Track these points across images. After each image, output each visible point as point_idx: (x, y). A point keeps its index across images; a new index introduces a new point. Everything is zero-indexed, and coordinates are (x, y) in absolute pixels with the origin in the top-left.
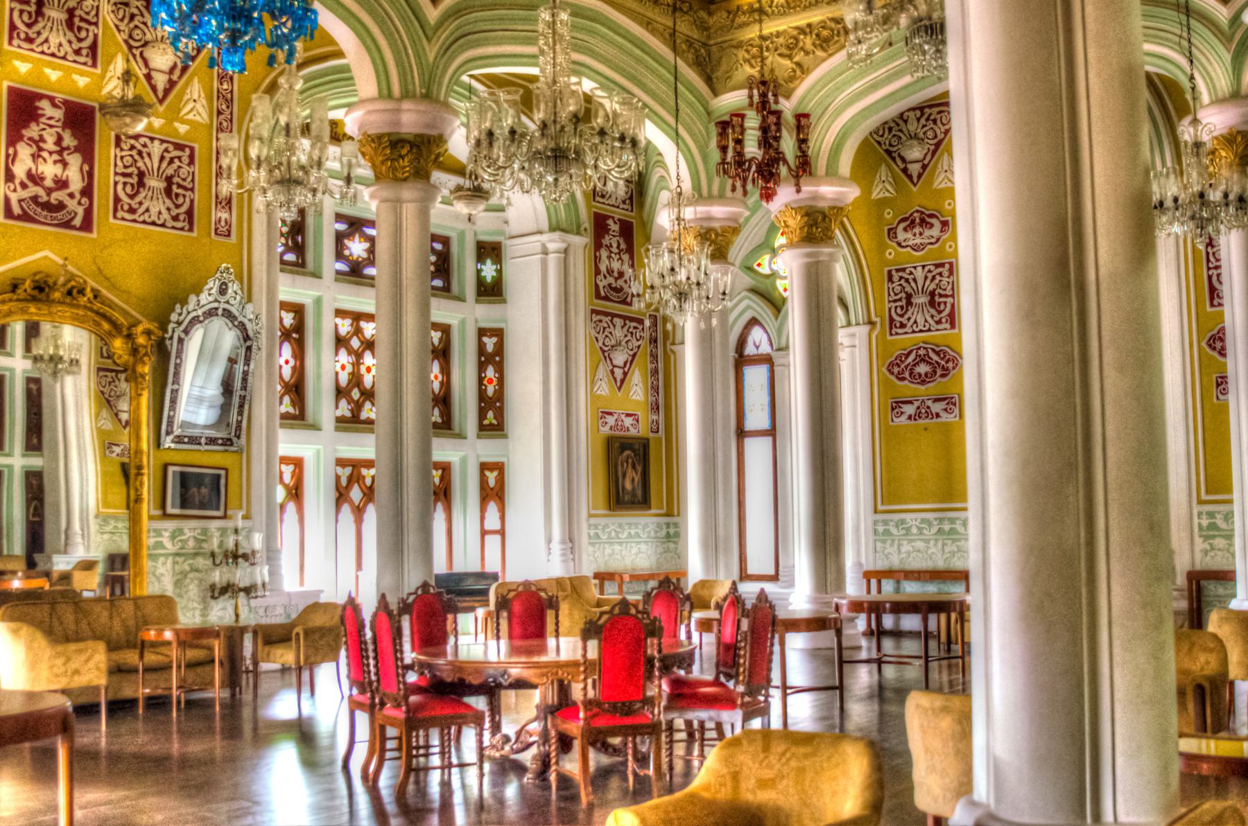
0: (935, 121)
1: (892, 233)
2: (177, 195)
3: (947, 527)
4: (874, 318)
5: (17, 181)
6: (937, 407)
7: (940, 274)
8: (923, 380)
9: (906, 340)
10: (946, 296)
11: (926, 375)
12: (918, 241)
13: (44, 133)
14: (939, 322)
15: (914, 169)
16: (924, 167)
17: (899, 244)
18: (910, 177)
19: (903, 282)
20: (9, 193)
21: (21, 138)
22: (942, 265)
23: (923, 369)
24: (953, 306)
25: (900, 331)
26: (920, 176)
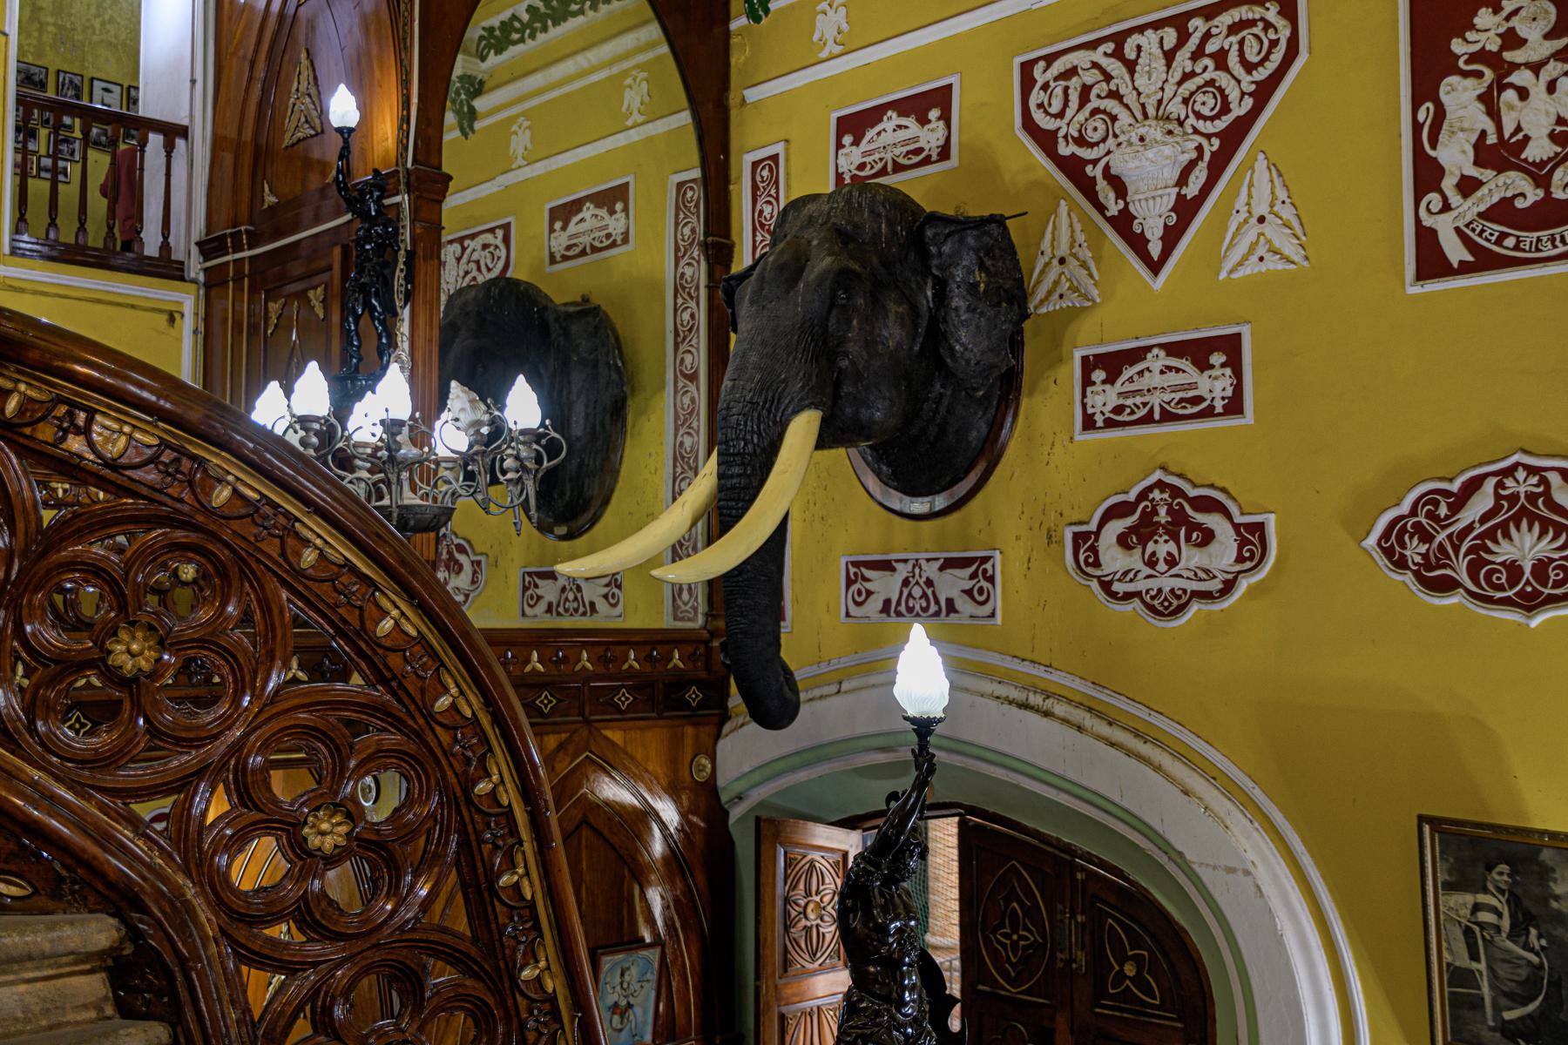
5: (1448, 184)
11: (1541, 568)
13: (1514, 22)
20: (1428, 221)
21: (1450, 66)
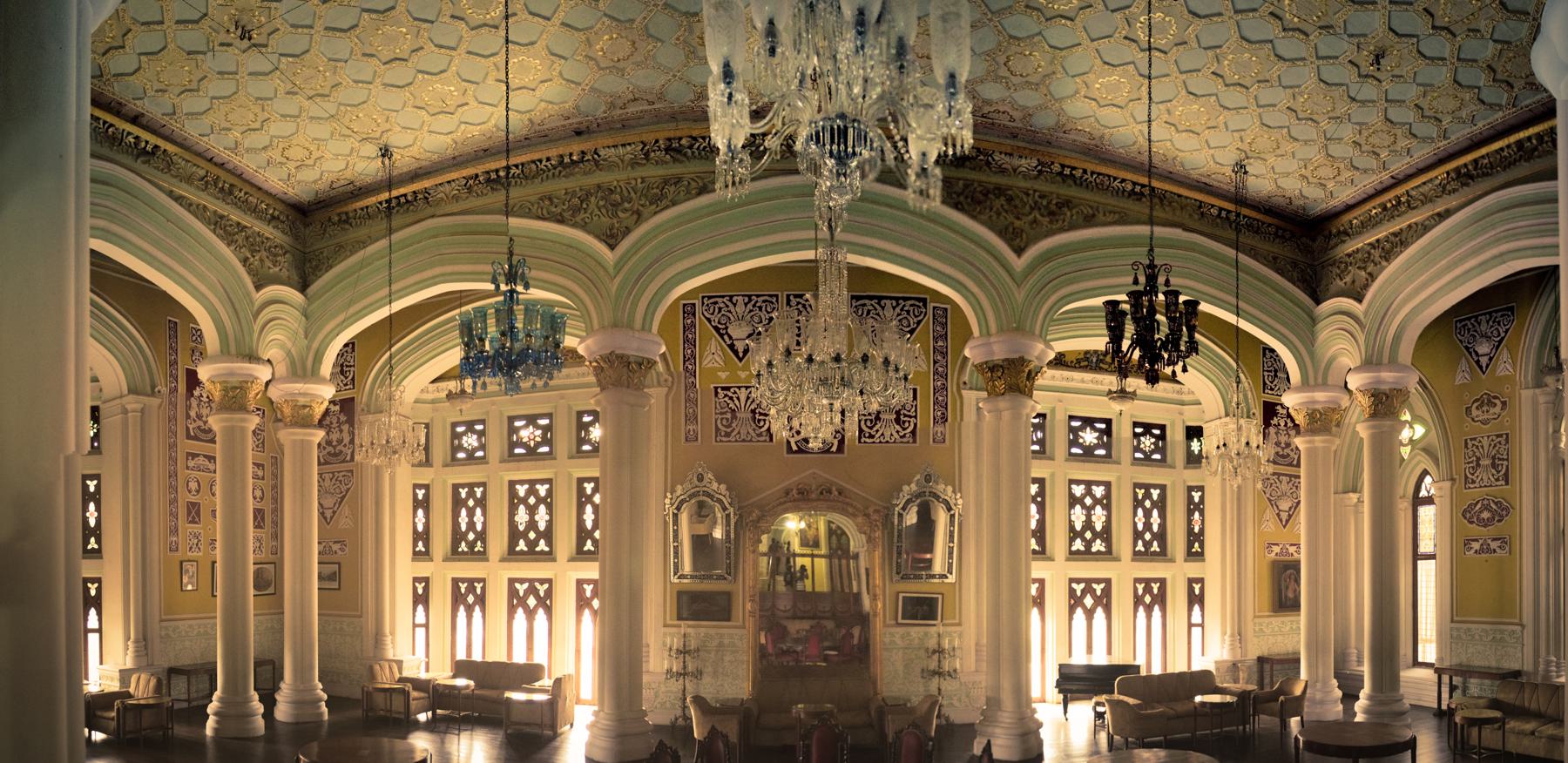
0: (1499, 323)
1: (1468, 410)
2: (904, 422)
3: (1498, 637)
4: (1455, 477)
6: (1494, 545)
7: (1500, 443)
8: (1486, 523)
9: (1476, 493)
10: (1503, 460)
12: (1486, 417)
14: (1497, 480)
15: (1484, 361)
16: (1491, 359)
17: (1473, 419)
18: (1481, 367)
19: (1474, 448)
22: (1501, 436)
23: (1486, 515)
24: (1507, 467)
25: (1472, 486)
26: (1487, 366)
